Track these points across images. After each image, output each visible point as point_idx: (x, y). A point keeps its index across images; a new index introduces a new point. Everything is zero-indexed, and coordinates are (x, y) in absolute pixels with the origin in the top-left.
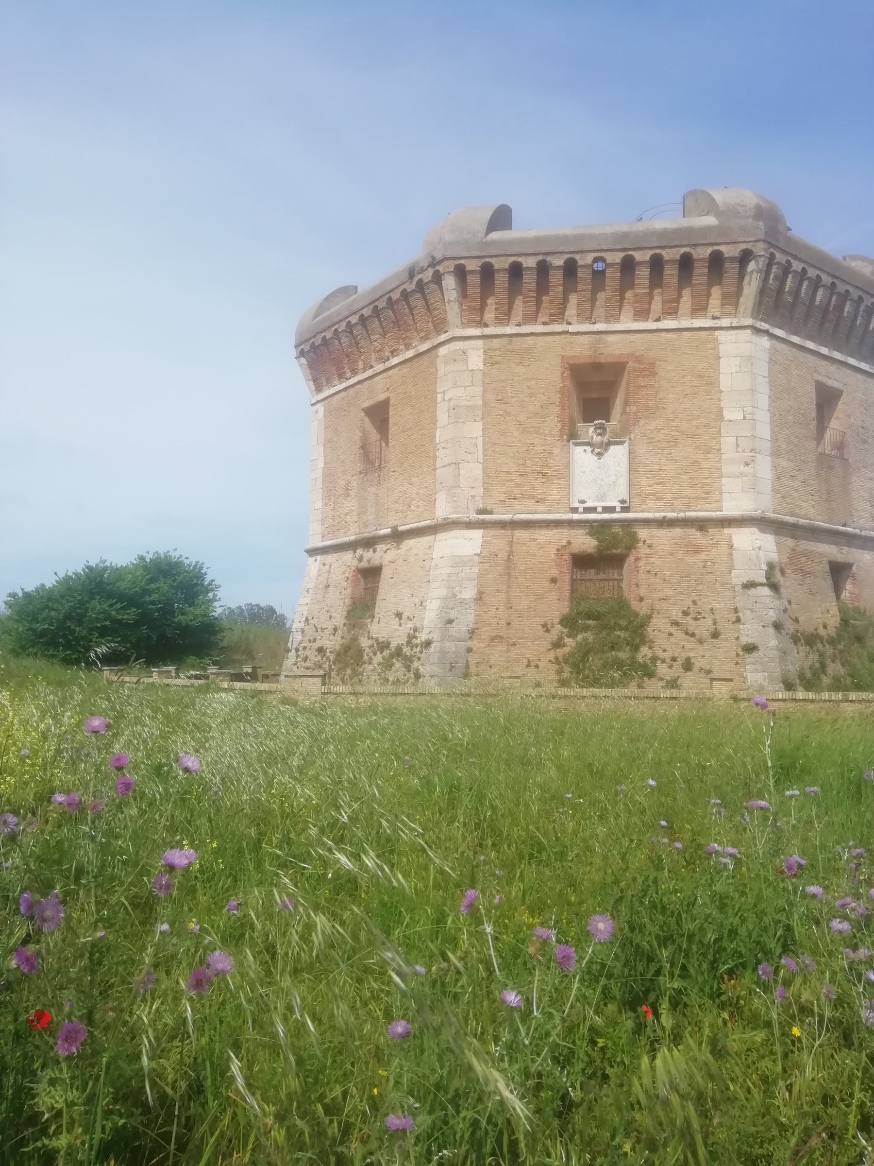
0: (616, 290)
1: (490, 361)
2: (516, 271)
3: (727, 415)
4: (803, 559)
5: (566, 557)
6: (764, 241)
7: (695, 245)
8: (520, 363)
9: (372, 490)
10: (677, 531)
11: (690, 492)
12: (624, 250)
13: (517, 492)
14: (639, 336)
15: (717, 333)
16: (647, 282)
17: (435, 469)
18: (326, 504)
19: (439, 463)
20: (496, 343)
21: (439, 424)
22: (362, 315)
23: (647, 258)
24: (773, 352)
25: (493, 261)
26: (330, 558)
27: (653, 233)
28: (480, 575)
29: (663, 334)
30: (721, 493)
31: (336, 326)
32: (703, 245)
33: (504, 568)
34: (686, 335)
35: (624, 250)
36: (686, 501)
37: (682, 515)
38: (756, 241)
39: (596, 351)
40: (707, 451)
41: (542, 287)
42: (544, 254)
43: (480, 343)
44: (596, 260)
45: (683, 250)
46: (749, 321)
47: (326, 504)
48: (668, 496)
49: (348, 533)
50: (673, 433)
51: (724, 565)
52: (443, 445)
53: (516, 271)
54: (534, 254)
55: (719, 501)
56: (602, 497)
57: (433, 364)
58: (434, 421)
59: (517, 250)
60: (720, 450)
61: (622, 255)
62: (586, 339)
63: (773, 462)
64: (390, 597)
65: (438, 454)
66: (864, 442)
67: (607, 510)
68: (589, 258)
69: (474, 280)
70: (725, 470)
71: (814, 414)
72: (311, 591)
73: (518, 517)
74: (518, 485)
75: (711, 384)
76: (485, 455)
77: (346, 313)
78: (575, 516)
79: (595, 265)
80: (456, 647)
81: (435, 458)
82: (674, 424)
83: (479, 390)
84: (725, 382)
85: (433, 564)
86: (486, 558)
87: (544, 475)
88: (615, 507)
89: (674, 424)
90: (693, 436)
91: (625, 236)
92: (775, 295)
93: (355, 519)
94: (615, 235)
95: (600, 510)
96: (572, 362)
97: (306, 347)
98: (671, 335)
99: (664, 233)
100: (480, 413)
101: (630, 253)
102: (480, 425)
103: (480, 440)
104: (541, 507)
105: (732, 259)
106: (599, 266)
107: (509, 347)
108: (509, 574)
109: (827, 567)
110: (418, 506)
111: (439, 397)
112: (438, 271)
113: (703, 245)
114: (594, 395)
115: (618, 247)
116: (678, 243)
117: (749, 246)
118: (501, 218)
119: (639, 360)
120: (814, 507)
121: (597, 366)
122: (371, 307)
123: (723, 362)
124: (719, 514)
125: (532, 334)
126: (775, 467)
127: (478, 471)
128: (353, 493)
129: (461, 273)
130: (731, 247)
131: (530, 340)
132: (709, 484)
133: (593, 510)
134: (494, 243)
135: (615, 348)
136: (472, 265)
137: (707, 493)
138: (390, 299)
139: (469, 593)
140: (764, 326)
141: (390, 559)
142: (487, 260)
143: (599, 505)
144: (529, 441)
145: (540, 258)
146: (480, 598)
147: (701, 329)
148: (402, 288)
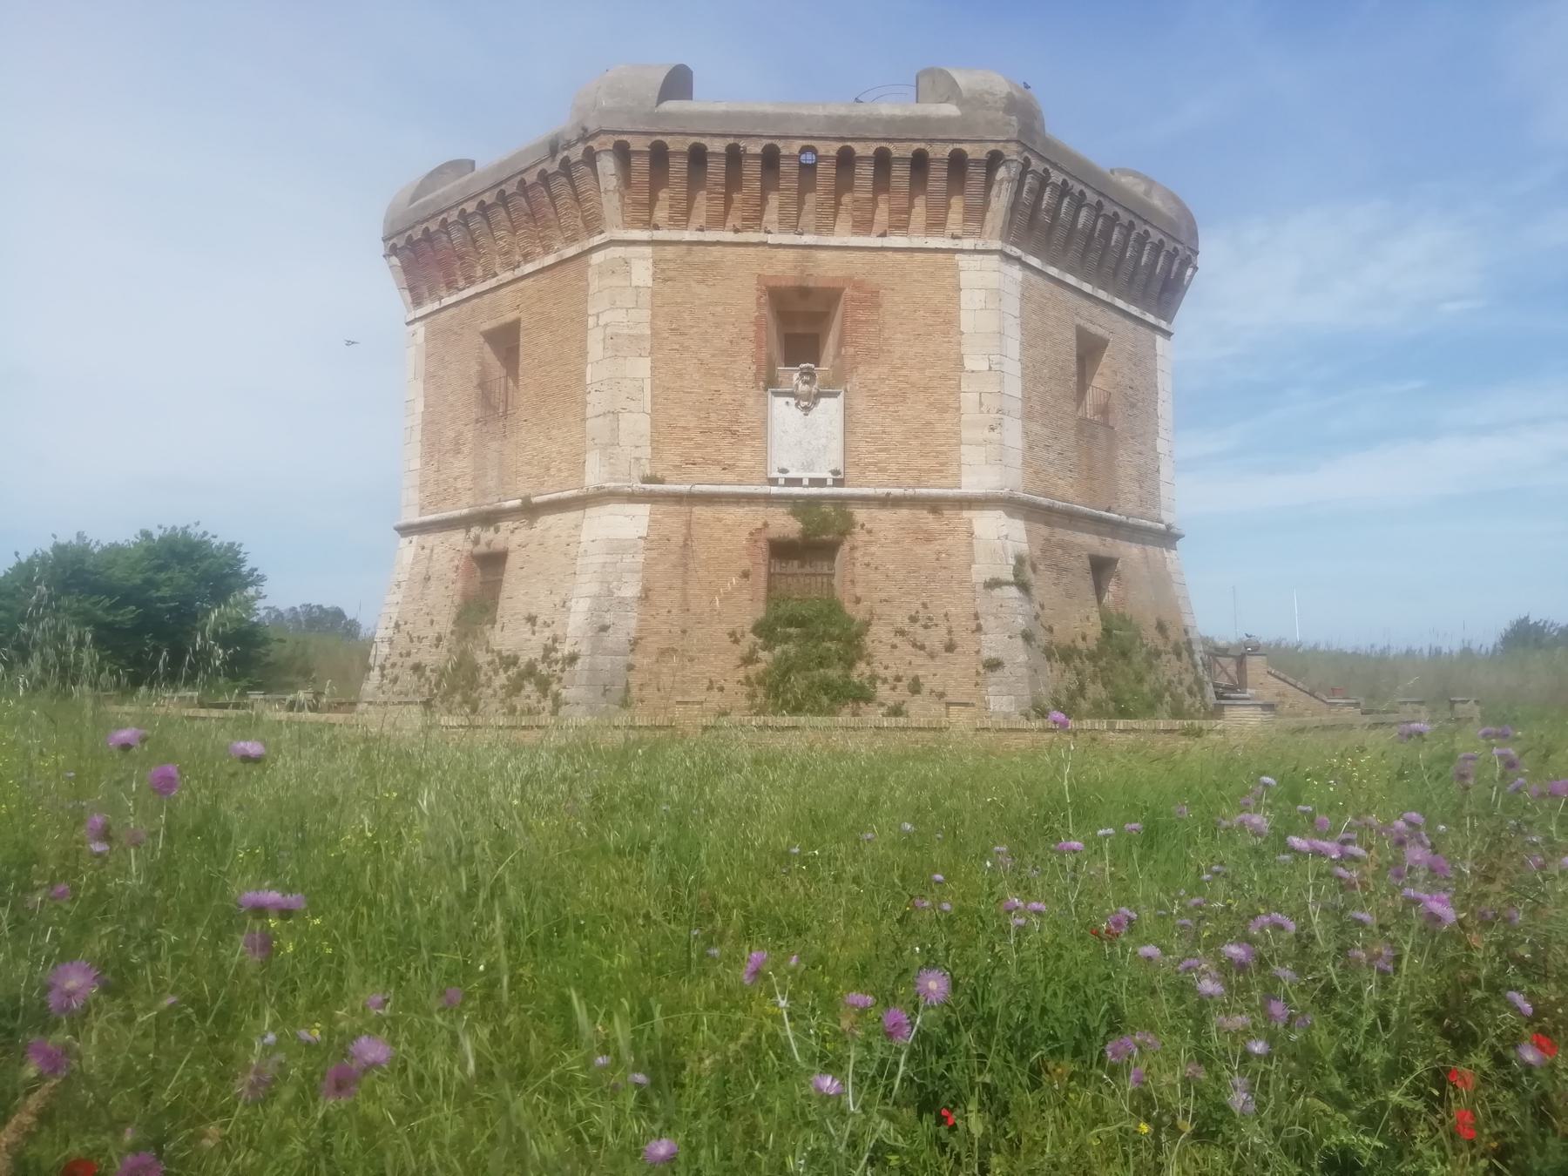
1: (662, 275)
2: (698, 156)
3: (969, 364)
4: (1059, 551)
6: (1018, 141)
7: (932, 141)
8: (703, 281)
9: (494, 445)
10: (904, 513)
13: (697, 454)
15: (957, 257)
16: (870, 183)
17: (584, 420)
19: (590, 411)
20: (670, 252)
21: (590, 358)
22: (482, 202)
23: (871, 153)
24: (1026, 287)
25: (667, 140)
26: (431, 539)
28: (647, 565)
29: (889, 254)
30: (959, 466)
33: (676, 558)
34: (919, 256)
36: (915, 473)
37: (910, 492)
39: (802, 271)
40: (944, 410)
41: (734, 180)
42: (736, 136)
43: (648, 250)
44: (804, 150)
45: (916, 146)
46: (997, 244)
48: (894, 467)
52: (597, 387)
55: (958, 475)
56: (808, 466)
57: (582, 277)
58: (583, 353)
60: (958, 409)
62: (791, 254)
64: (517, 594)
65: (589, 398)
66: (1133, 406)
67: (815, 482)
68: (796, 146)
69: (641, 165)
70: (966, 434)
71: (1073, 368)
73: (698, 488)
74: (698, 446)
75: (950, 322)
76: (654, 404)
78: (774, 490)
80: (612, 663)
81: (585, 404)
82: (903, 372)
83: (646, 314)
84: (967, 321)
85: (581, 550)
86: (654, 542)
87: (734, 433)
89: (903, 372)
90: (926, 389)
91: (842, 120)
93: (469, 484)
95: (806, 482)
96: (771, 284)
97: (401, 242)
98: (899, 256)
99: (891, 121)
100: (648, 346)
102: (647, 362)
103: (648, 382)
104: (729, 477)
105: (977, 162)
106: (808, 158)
107: (688, 259)
108: (685, 565)
109: (1087, 564)
110: (560, 470)
111: (591, 321)
112: (591, 148)
114: (799, 330)
117: (999, 147)
118: (678, 83)
119: (858, 286)
121: (804, 292)
122: (496, 191)
124: (956, 491)
125: (717, 243)
126: (1026, 433)
127: (643, 424)
128: (466, 450)
129: (623, 153)
130: (976, 146)
131: (716, 252)
133: (797, 482)
134: (668, 116)
135: (828, 268)
136: (639, 144)
137: (942, 465)
138: (522, 182)
139: (631, 590)
143: (806, 476)
144: (713, 387)
145: (731, 141)
146: (645, 596)
147: (937, 250)
148: (540, 168)
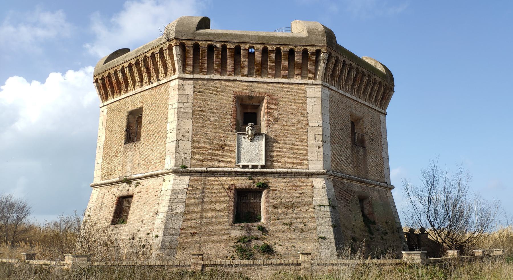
0: (259, 63)
1: (197, 91)
2: (211, 49)
3: (311, 124)
4: (346, 194)
5: (233, 191)
6: (326, 46)
7: (296, 46)
8: (213, 93)
9: (131, 153)
10: (287, 179)
11: (295, 160)
12: (264, 44)
13: (209, 156)
14: (271, 85)
15: (306, 86)
16: (274, 60)
17: (165, 144)
18: (104, 161)
19: (168, 140)
20: (200, 82)
21: (169, 120)
22: (130, 63)
23: (274, 49)
24: (331, 96)
25: (199, 42)
26: (105, 189)
27: (276, 38)
28: (187, 200)
29: (281, 85)
30: (308, 161)
31: (116, 68)
32: (300, 45)
33: (197, 197)
34: (292, 86)
35: (264, 44)
36: (291, 164)
37: (289, 170)
38: (323, 46)
39: (250, 90)
40: (301, 141)
41: (264, 62)
42: (225, 42)
43: (192, 82)
44: (250, 47)
45: (290, 47)
46: (320, 82)
47: (104, 161)
48: (283, 161)
49: (116, 177)
50: (286, 131)
51: (309, 196)
52: (171, 131)
53: (211, 49)
54: (220, 42)
55: (307, 165)
56: (251, 161)
57: (167, 90)
58: (166, 119)
59: (211, 38)
60: (307, 140)
61: (262, 46)
62: (245, 84)
63: (331, 147)
64: (135, 211)
65: (168, 135)
66: (373, 140)
67: (254, 167)
68: (247, 46)
69: (189, 52)
70: (310, 150)
71: (350, 126)
72: (92, 208)
73: (209, 169)
74: (209, 153)
75: (303, 109)
76: (193, 138)
77: (122, 62)
78: (239, 170)
79: (250, 50)
80: (171, 239)
81: (166, 137)
82: (286, 127)
83: (190, 105)
84: (309, 109)
85: (162, 194)
86: (191, 190)
87: (223, 148)
88: (258, 166)
89: (286, 127)
90: (295, 133)
91: (264, 37)
92: (332, 71)
93: (120, 168)
94: (259, 37)
95: (250, 167)
96: (238, 94)
97: (99, 77)
98: (285, 86)
99: (282, 38)
100: (191, 116)
101: (266, 46)
102: (191, 122)
103: (191, 129)
104: (221, 165)
105: (312, 53)
106: (252, 51)
107: (207, 85)
108: (203, 199)
109: (358, 198)
110: (155, 163)
111: (170, 107)
112: (171, 45)
113: (300, 45)
114: (249, 111)
115: (260, 42)
116: (288, 43)
117: (320, 48)
118: (205, 23)
119: (269, 96)
120: (350, 169)
121: (250, 98)
122: (136, 59)
123: (309, 100)
124: (307, 171)
125: (218, 80)
126: (332, 149)
127: (189, 145)
128: (120, 155)
129: (183, 47)
130: (312, 48)
131: (218, 83)
132: (302, 156)
133: (247, 167)
134: (200, 34)
135: (259, 89)
136: (188, 43)
137: (301, 160)
138: (146, 56)
139: (180, 210)
140: (327, 84)
141: (138, 191)
142: (197, 42)
143: (250, 164)
144: (216, 132)
145: (223, 43)
146: (187, 210)
147: (298, 84)
148: (152, 51)
